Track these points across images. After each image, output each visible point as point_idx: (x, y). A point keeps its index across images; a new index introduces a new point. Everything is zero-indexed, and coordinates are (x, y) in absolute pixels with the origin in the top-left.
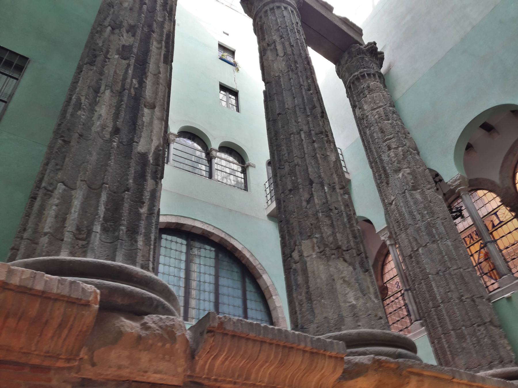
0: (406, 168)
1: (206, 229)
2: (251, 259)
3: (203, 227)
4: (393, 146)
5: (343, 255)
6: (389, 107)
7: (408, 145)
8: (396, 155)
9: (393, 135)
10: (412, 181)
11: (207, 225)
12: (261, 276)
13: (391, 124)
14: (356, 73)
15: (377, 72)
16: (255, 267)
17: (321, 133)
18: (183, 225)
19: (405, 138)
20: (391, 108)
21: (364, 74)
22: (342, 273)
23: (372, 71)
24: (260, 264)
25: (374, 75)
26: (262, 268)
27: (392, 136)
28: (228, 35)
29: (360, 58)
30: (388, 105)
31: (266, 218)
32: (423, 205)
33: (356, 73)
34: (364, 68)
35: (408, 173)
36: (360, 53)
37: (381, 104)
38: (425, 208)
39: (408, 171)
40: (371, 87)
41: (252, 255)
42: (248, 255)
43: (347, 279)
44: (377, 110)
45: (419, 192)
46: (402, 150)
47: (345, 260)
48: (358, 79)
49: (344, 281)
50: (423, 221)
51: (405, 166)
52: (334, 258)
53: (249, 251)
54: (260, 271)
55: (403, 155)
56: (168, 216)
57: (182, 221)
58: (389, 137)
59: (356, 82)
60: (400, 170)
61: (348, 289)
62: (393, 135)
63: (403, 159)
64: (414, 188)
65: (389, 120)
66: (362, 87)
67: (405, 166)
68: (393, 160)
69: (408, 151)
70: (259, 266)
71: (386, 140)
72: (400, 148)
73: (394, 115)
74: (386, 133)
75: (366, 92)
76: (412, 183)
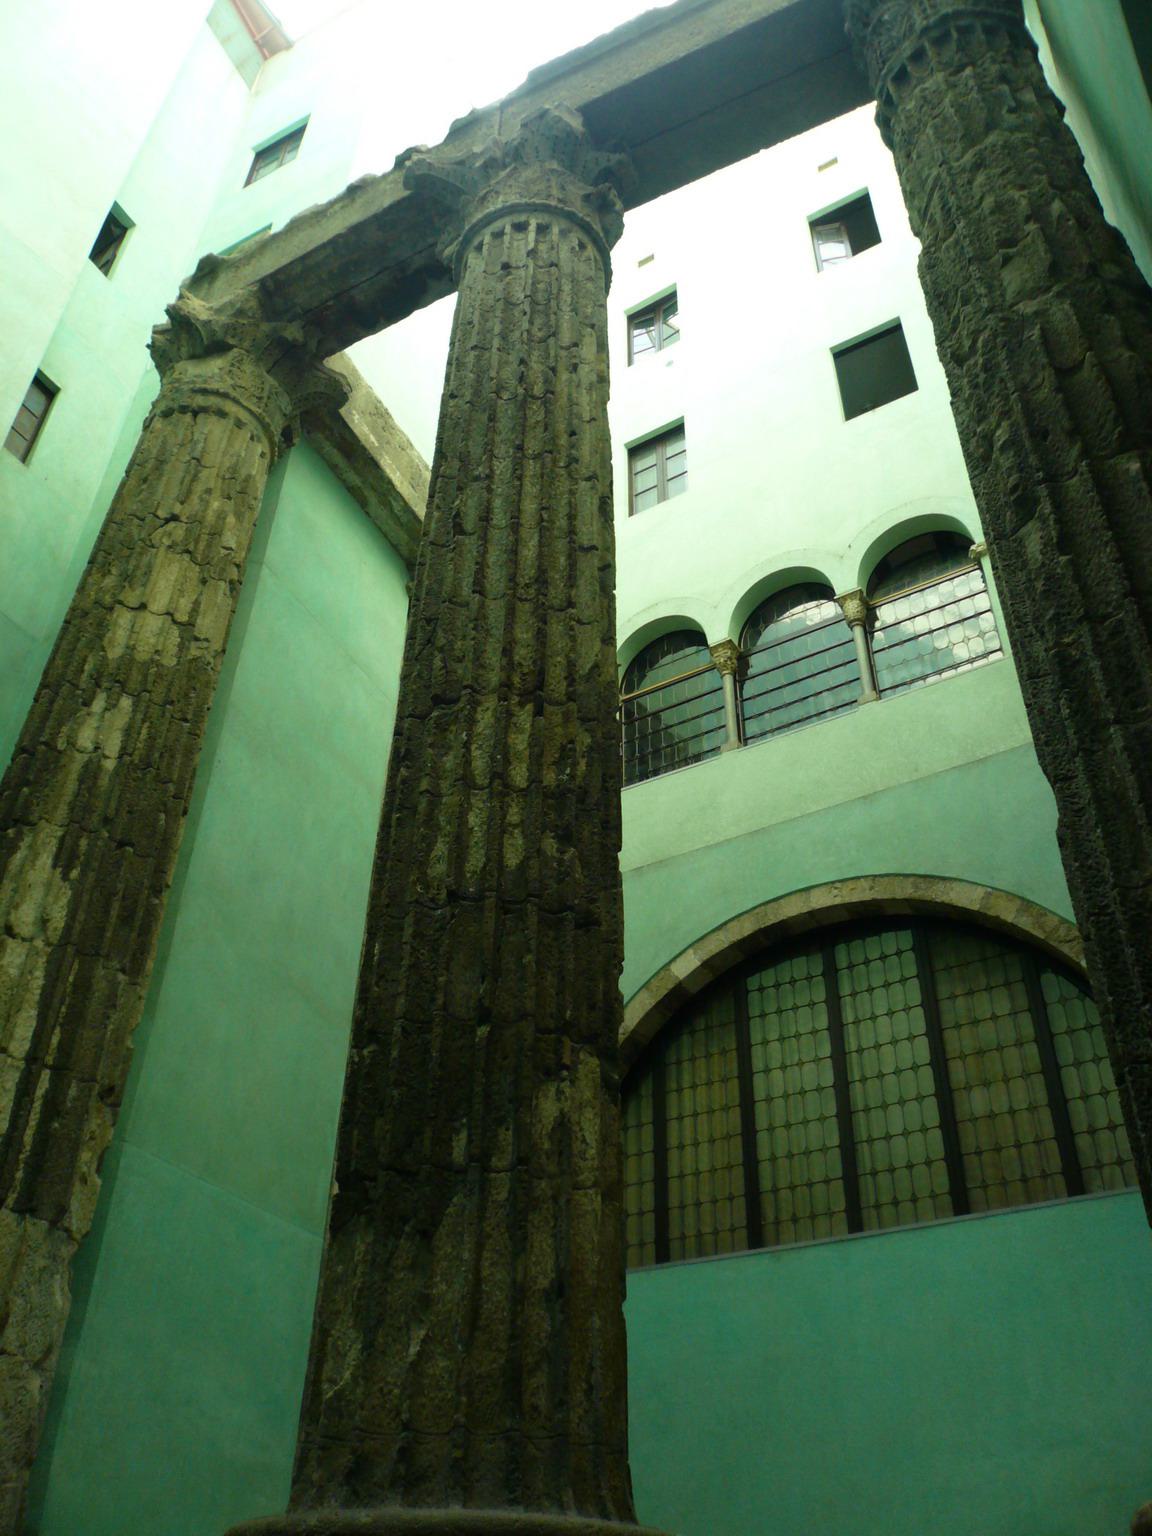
0: (998, 425)
1: (847, 900)
2: (1025, 923)
3: (838, 901)
11: (851, 885)
15: (925, 30)
18: (782, 925)
19: (1007, 260)
23: (907, 48)
25: (918, 56)
28: (835, 161)
36: (867, 16)
41: (1027, 905)
53: (1011, 896)
56: (729, 925)
57: (772, 919)
70: (1062, 932)
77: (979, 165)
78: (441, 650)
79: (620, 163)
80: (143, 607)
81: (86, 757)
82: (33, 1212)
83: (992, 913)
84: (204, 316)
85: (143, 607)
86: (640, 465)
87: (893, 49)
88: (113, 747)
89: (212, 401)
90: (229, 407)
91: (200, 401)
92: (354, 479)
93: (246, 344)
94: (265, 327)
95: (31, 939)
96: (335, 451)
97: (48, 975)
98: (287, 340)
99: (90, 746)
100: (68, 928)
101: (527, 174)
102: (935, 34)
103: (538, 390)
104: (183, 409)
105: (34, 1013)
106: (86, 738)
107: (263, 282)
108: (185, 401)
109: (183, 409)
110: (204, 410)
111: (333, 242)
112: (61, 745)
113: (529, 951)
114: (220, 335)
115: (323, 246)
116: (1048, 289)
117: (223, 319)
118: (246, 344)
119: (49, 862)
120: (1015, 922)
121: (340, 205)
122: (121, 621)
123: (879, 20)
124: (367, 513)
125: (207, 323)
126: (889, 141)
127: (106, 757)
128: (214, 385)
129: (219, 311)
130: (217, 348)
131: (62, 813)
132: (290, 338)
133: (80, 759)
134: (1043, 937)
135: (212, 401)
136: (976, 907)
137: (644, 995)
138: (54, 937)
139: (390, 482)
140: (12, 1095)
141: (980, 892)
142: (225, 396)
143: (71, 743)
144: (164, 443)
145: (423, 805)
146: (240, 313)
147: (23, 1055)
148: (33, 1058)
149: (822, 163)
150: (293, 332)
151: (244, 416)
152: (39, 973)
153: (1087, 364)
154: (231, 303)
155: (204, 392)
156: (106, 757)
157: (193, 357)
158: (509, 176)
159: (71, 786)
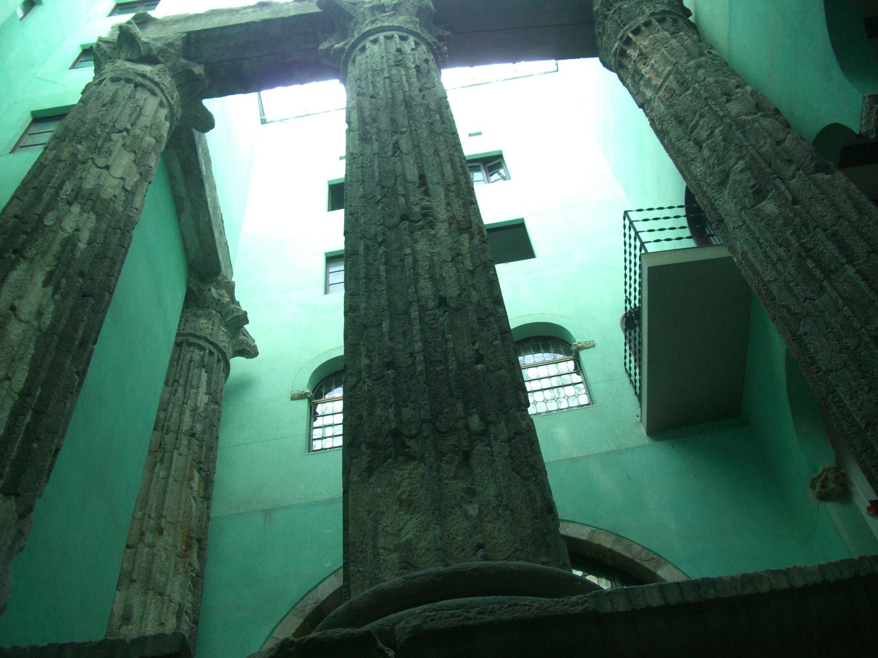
0: (736, 163)
4: (705, 134)
5: (404, 446)
6: (688, 61)
7: (733, 113)
8: (713, 150)
9: (698, 113)
10: (752, 182)
12: (655, 574)
13: (691, 94)
14: (616, 45)
15: (652, 14)
16: (632, 560)
17: (404, 217)
19: (728, 101)
20: (692, 62)
21: (628, 37)
22: (398, 488)
23: (641, 20)
24: (644, 548)
25: (647, 24)
26: (651, 555)
27: (697, 118)
28: (480, 134)
29: (614, 13)
30: (685, 59)
31: (647, 440)
32: (780, 222)
33: (616, 45)
34: (625, 25)
35: (742, 171)
36: (611, 5)
37: (669, 68)
38: (787, 222)
39: (741, 165)
40: (644, 50)
41: (619, 538)
42: (607, 542)
43: (404, 497)
44: (667, 83)
45: (772, 197)
46: (721, 131)
47: (413, 458)
48: (623, 53)
49: (401, 503)
50: (790, 258)
51: (732, 161)
52: (390, 464)
53: (609, 533)
54: (646, 565)
55: (724, 140)
58: (694, 122)
59: (625, 62)
60: (728, 176)
61: (408, 517)
62: (698, 113)
63: (725, 148)
64: (759, 194)
65: (688, 89)
66: (632, 63)
67: (732, 161)
68: (711, 161)
69: (731, 125)
71: (691, 132)
72: (717, 131)
73: (701, 72)
74: (688, 119)
75: (640, 66)
76: (752, 187)
77: (699, 66)
78: (403, 195)
79: (449, 36)
80: (107, 167)
81: (67, 235)
82: (17, 495)
83: (596, 542)
84: (144, 39)
85: (107, 167)
86: (331, 270)
87: (631, 19)
88: (85, 235)
89: (148, 83)
90: (158, 91)
91: (139, 79)
92: (182, 190)
93: (169, 64)
94: (183, 61)
95: (27, 322)
96: (179, 166)
97: (36, 348)
98: (193, 73)
99: (70, 230)
100: (53, 326)
101: (401, 18)
102: (658, 17)
103: (433, 106)
104: (128, 81)
105: (26, 368)
106: (69, 225)
107: (189, 33)
108: (131, 77)
109: (128, 81)
110: (143, 86)
111: (247, 25)
112: (49, 221)
113: (496, 339)
114: (155, 53)
115: (240, 25)
116: (755, 114)
117: (159, 44)
118: (169, 64)
119: (40, 284)
120: (612, 548)
121: (251, 10)
122: (91, 171)
123: (619, 8)
124: (179, 220)
125: (145, 43)
126: (612, 71)
127: (79, 241)
128: (149, 75)
129: (154, 40)
130: (150, 59)
131: (50, 259)
132: (197, 72)
133: (62, 235)
134: (631, 557)
135: (148, 83)
136: (585, 538)
137: (333, 579)
138: (44, 328)
139: (206, 201)
140: (7, 413)
141: (587, 530)
142: (157, 84)
143: (59, 220)
144: (116, 92)
145: (410, 259)
146: (170, 45)
147: (18, 391)
148: (25, 394)
149: (472, 132)
150: (198, 70)
151: (165, 102)
152: (31, 345)
153: (787, 140)
154: (165, 38)
155: (144, 76)
156: (79, 241)
157: (129, 60)
158: (391, 16)
159: (56, 247)
